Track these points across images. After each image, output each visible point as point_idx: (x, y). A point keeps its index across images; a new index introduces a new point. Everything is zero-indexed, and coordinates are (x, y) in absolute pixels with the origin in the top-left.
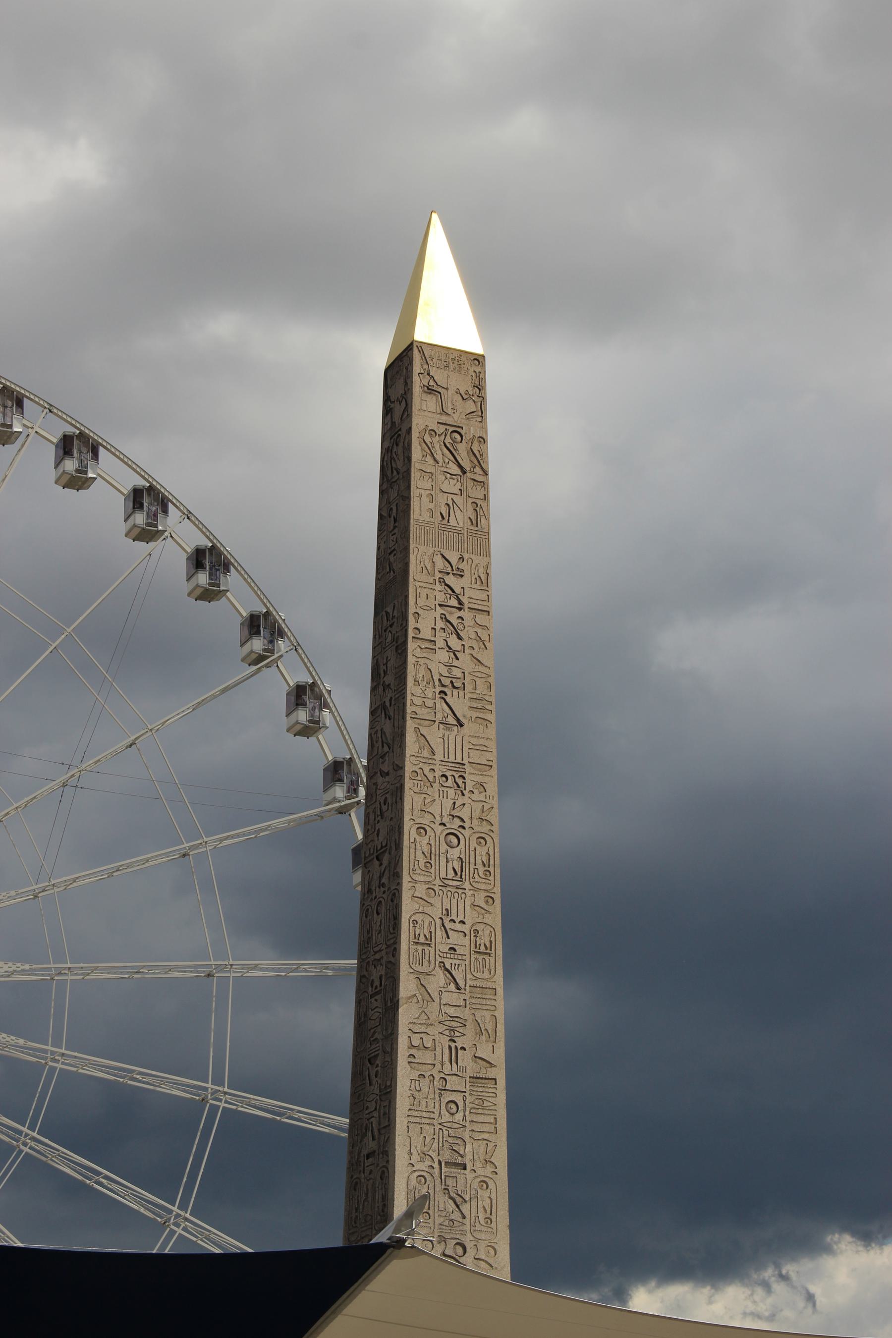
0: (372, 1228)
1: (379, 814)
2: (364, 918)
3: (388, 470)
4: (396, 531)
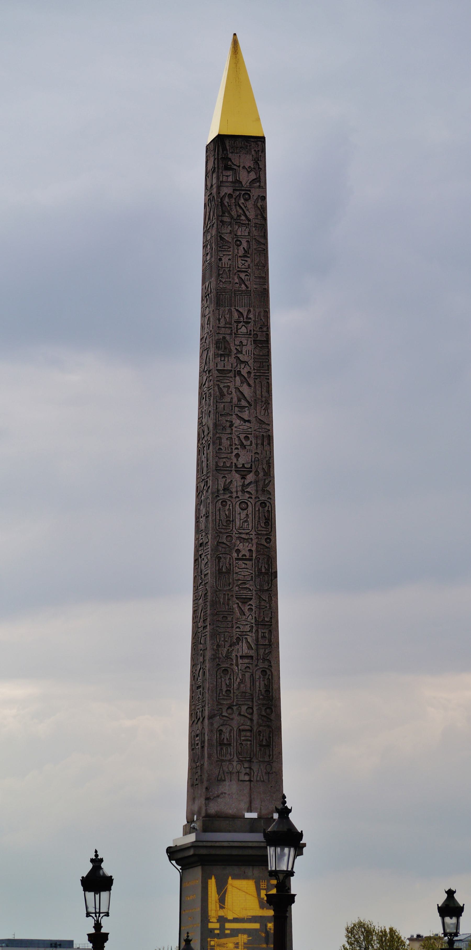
0: (253, 701)
1: (237, 442)
2: (219, 505)
3: (231, 209)
4: (249, 260)
